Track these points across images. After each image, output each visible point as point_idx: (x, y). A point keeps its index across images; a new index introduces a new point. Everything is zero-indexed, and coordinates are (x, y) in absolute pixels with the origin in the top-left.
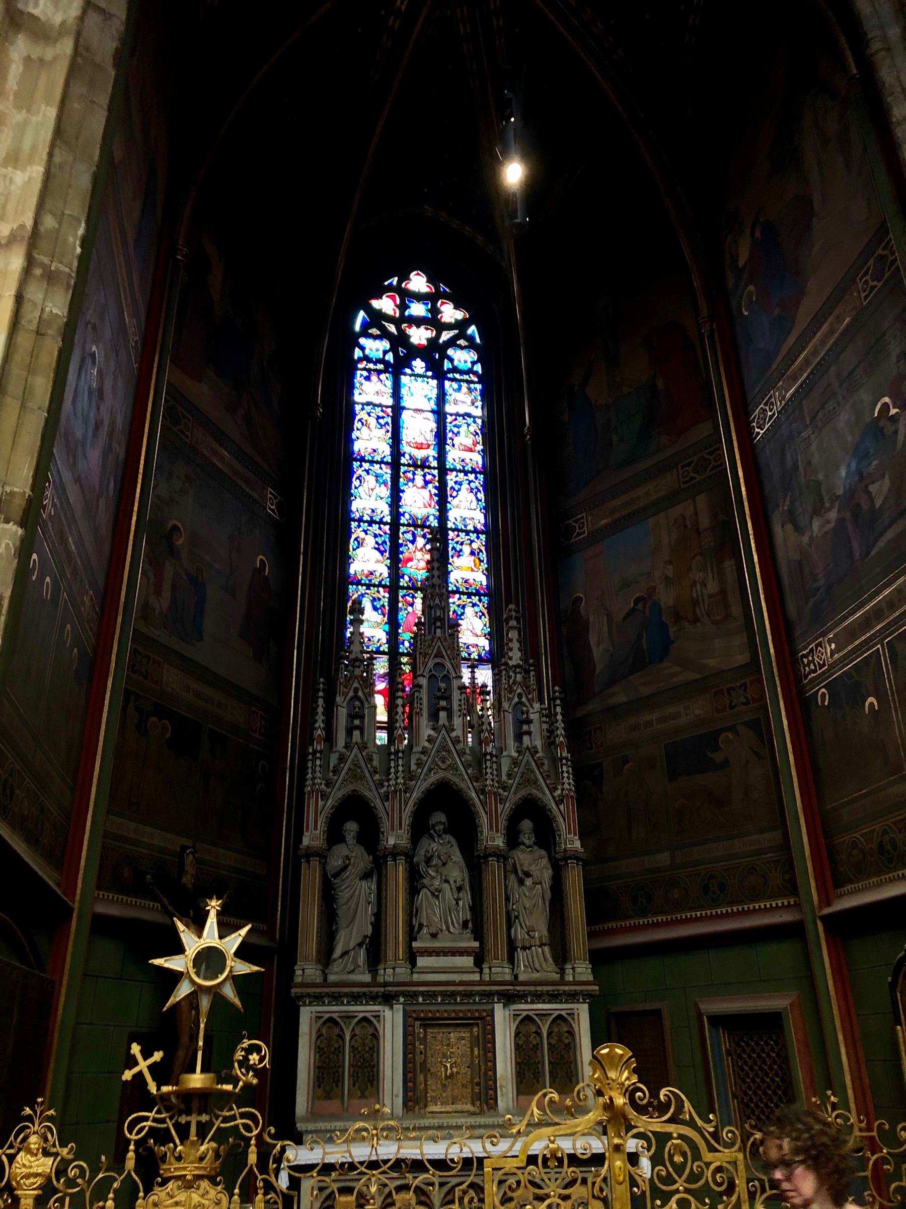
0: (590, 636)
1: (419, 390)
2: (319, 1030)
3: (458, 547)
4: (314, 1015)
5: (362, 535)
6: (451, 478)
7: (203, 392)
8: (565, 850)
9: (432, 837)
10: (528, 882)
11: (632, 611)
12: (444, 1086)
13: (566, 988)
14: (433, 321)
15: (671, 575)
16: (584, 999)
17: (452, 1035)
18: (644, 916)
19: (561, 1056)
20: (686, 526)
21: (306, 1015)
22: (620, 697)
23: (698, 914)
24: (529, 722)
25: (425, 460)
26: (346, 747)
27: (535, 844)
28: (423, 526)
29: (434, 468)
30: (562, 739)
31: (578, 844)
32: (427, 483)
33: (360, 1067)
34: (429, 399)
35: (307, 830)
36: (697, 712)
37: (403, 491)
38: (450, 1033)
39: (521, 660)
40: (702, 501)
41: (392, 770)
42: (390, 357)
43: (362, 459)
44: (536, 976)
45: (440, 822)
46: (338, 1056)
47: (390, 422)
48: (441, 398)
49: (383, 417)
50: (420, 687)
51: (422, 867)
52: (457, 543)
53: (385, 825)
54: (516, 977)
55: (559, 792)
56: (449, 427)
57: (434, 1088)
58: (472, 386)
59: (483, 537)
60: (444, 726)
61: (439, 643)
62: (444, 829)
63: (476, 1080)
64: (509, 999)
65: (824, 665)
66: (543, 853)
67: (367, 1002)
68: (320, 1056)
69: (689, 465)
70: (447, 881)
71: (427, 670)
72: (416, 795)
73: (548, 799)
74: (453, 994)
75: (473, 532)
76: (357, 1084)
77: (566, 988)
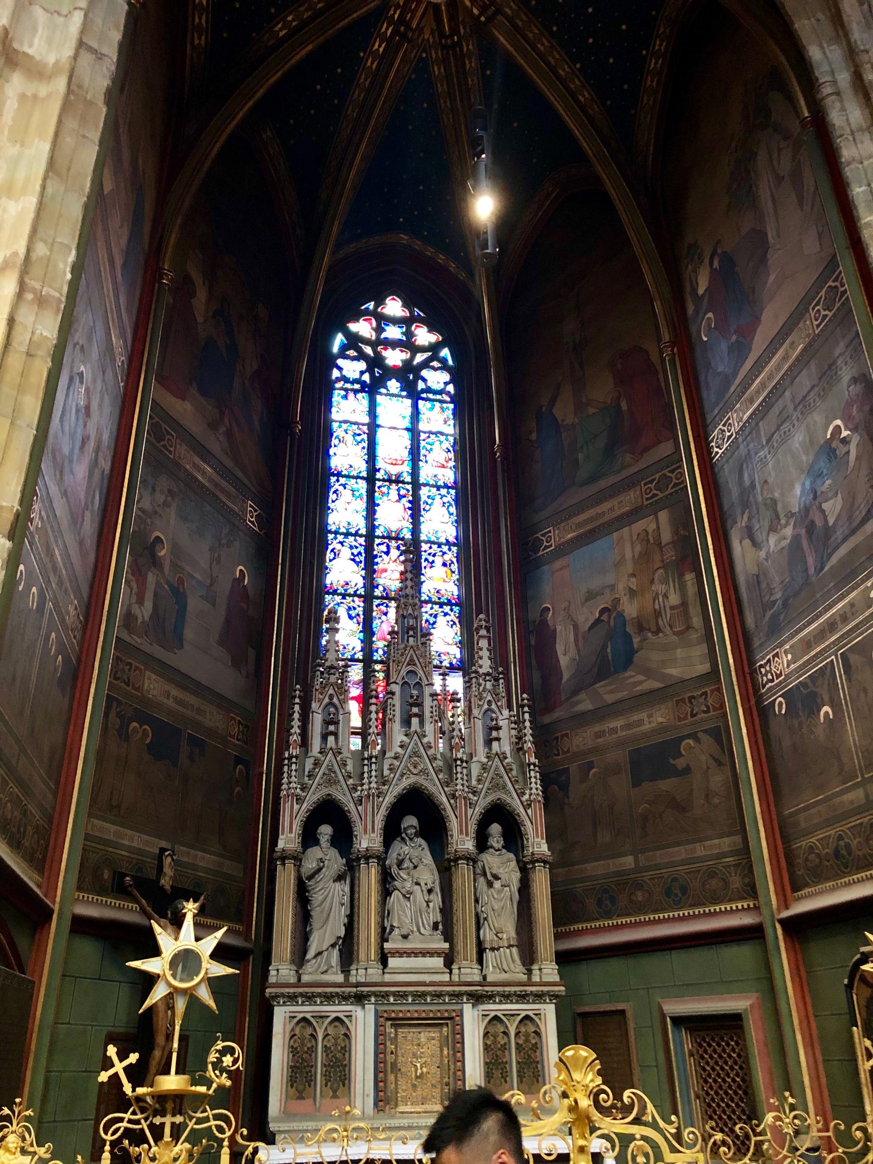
0: (557, 646)
1: (393, 408)
2: (293, 1030)
3: (431, 559)
4: (288, 1015)
5: (339, 546)
6: (424, 492)
7: (185, 410)
8: (533, 854)
9: (403, 839)
10: (497, 884)
11: (598, 621)
12: (414, 1086)
13: (534, 989)
14: (408, 344)
15: (635, 588)
16: (550, 1000)
17: (422, 1034)
18: (610, 918)
20: (648, 541)
21: (280, 1014)
22: (585, 704)
23: (661, 916)
24: (498, 728)
25: (399, 475)
26: (320, 753)
27: (503, 847)
28: (397, 539)
29: (408, 483)
30: (530, 745)
31: (544, 847)
32: (401, 497)
33: (332, 1067)
34: (404, 417)
35: (283, 834)
36: (660, 720)
37: (378, 505)
38: (420, 1033)
39: (491, 668)
40: (664, 516)
41: (366, 775)
42: (366, 377)
43: (339, 475)
44: (504, 977)
45: (412, 826)
46: (310, 1055)
47: (366, 439)
48: (416, 414)
49: (359, 435)
50: (393, 694)
51: (394, 870)
52: (429, 554)
53: (358, 829)
54: (485, 977)
55: (526, 797)
56: (422, 444)
57: (404, 1088)
58: (445, 405)
59: (454, 549)
60: (416, 732)
61: (412, 652)
62: (415, 833)
63: (446, 1080)
64: (477, 999)
65: (781, 675)
66: (512, 856)
67: (339, 1002)
68: (293, 1056)
69: (651, 482)
70: (418, 884)
71: (400, 677)
72: (389, 799)
73: (516, 804)
74: (423, 995)
75: (445, 545)
76: (329, 1084)
77: (534, 989)
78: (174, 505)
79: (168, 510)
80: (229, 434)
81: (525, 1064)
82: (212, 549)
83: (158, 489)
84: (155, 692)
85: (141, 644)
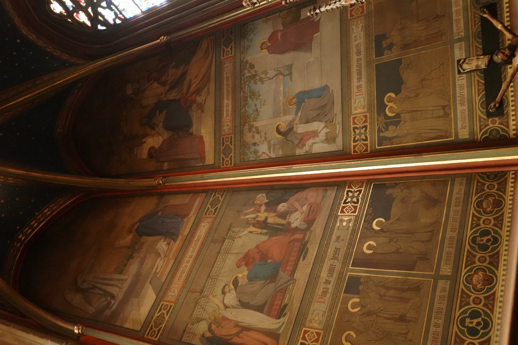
78: (256, 124)
79: (259, 128)
80: (198, 92)
82: (262, 81)
83: (253, 141)
84: (362, 100)
85: (339, 124)
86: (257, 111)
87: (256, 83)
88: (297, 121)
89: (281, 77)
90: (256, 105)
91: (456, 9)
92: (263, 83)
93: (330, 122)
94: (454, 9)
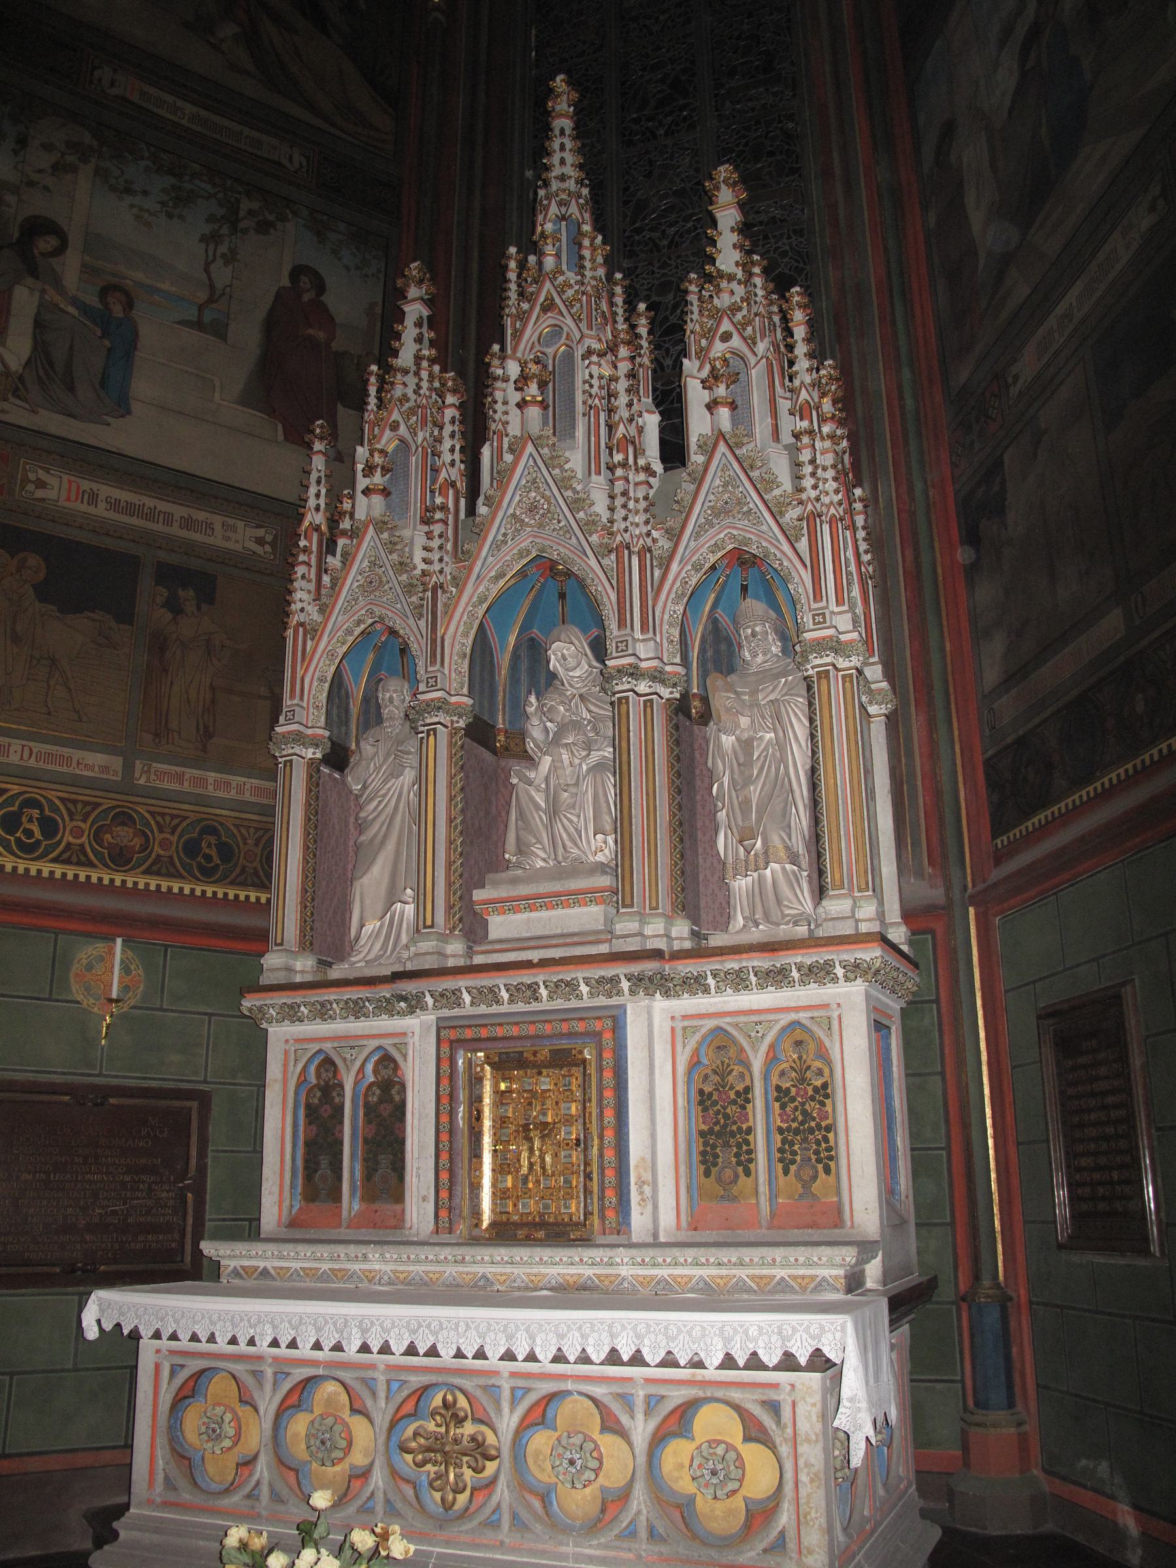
19: (805, 1113)
81: (797, 1132)
82: (212, 238)
86: (128, 191)
87: (210, 219)
88: (51, 295)
89: (203, 296)
90: (145, 193)
91: (211, 781)
92: (204, 239)
93: (17, 389)
94: (212, 776)
